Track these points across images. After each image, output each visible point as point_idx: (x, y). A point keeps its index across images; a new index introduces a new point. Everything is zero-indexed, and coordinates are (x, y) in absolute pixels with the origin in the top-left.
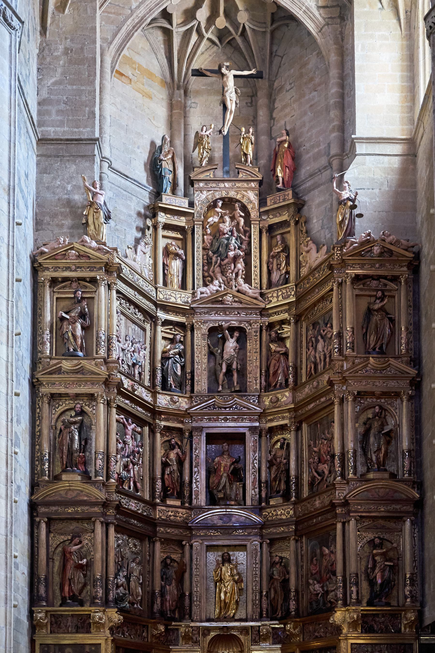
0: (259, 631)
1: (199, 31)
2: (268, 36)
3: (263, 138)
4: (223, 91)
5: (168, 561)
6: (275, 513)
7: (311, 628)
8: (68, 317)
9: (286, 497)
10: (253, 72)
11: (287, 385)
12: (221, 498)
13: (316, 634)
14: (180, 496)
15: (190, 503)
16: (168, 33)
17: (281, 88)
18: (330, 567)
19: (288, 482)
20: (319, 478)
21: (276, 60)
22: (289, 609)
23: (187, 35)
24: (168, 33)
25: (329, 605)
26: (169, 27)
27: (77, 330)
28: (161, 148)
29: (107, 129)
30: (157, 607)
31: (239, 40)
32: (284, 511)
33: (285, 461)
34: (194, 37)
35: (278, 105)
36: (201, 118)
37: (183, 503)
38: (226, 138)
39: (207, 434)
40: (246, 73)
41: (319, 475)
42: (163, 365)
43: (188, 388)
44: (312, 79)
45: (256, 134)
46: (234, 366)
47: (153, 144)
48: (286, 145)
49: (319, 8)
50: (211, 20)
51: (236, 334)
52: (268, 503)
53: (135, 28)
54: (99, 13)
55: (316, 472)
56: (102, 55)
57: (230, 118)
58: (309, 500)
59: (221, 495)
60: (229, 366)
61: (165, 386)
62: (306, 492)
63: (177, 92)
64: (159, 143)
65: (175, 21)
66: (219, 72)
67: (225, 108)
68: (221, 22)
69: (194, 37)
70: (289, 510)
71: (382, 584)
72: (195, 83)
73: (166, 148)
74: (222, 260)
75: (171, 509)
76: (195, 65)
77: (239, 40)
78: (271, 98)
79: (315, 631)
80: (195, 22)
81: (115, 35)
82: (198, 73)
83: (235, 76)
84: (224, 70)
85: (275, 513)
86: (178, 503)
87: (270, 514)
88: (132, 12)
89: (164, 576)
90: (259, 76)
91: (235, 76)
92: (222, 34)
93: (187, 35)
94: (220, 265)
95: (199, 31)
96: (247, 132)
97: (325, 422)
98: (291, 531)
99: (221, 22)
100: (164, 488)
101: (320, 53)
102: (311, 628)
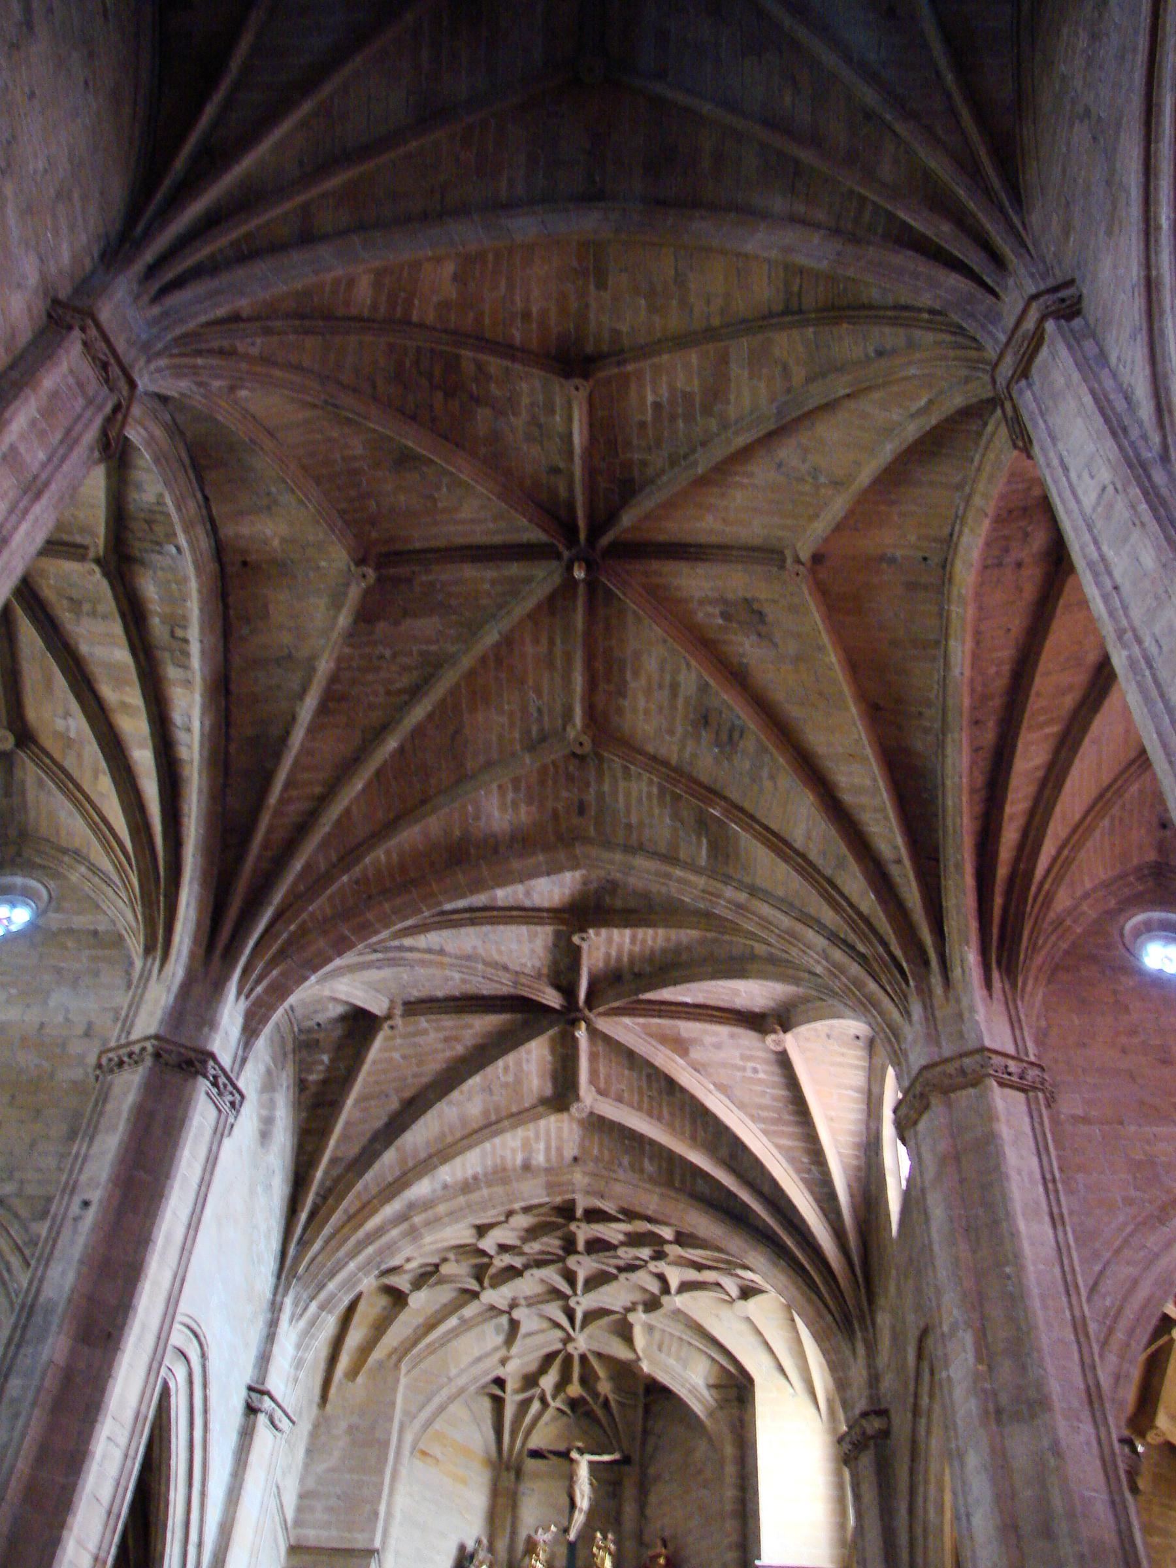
1: (543, 1400)
2: (640, 1411)
3: (630, 1544)
4: (571, 1478)
10: (616, 1456)
16: (498, 1403)
17: (658, 1478)
21: (651, 1441)
23: (525, 1405)
24: (498, 1403)
26: (499, 1392)
28: (472, 1556)
29: (395, 1531)
31: (600, 1413)
34: (536, 1406)
35: (653, 1499)
36: (535, 1515)
38: (572, 1546)
40: (606, 1458)
44: (700, 1472)
45: (617, 1542)
47: (462, 1548)
48: (662, 1561)
49: (710, 1387)
50: (560, 1386)
53: (452, 1399)
54: (403, 1380)
56: (401, 1431)
57: (579, 1518)
63: (505, 1473)
64: (470, 1545)
65: (510, 1386)
66: (565, 1455)
67: (573, 1505)
68: (575, 1389)
69: (536, 1406)
72: (531, 1464)
73: (482, 1555)
76: (535, 1442)
77: (600, 1413)
78: (643, 1491)
80: (537, 1391)
81: (422, 1407)
82: (536, 1454)
83: (590, 1463)
84: (574, 1455)
88: (450, 1380)
90: (626, 1460)
91: (590, 1463)
92: (574, 1404)
93: (525, 1405)
95: (543, 1400)
96: (605, 1538)
99: (575, 1389)
101: (710, 1440)
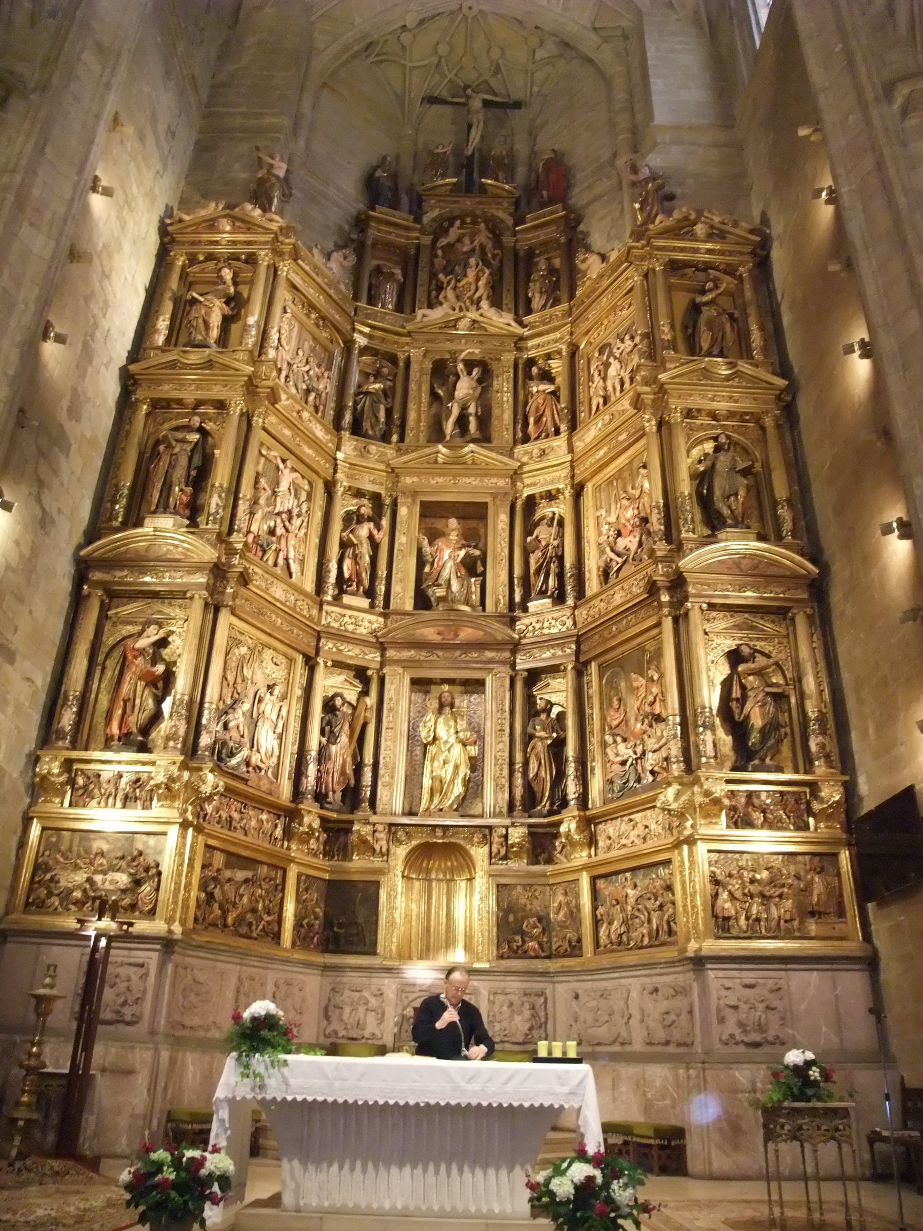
0: (506, 837)
5: (338, 702)
6: (538, 626)
7: (611, 830)
8: (202, 299)
9: (559, 599)
11: (557, 432)
12: (441, 599)
13: (623, 841)
14: (370, 593)
15: (387, 604)
18: (648, 709)
19: (560, 576)
20: (620, 560)
22: (566, 794)
25: (651, 778)
27: (214, 315)
30: (310, 781)
32: (556, 620)
33: (556, 543)
37: (372, 606)
39: (421, 502)
41: (619, 555)
42: (356, 403)
43: (395, 438)
46: (472, 409)
51: (475, 371)
52: (525, 610)
55: (613, 550)
58: (603, 597)
59: (440, 592)
60: (464, 408)
61: (357, 429)
62: (593, 585)
70: (564, 618)
71: (762, 731)
74: (459, 281)
75: (349, 612)
79: (620, 836)
85: (538, 626)
86: (364, 603)
87: (530, 628)
89: (327, 728)
94: (455, 288)
97: (626, 474)
98: (569, 655)
100: (340, 579)
102: (611, 830)
